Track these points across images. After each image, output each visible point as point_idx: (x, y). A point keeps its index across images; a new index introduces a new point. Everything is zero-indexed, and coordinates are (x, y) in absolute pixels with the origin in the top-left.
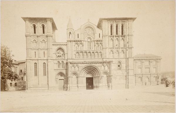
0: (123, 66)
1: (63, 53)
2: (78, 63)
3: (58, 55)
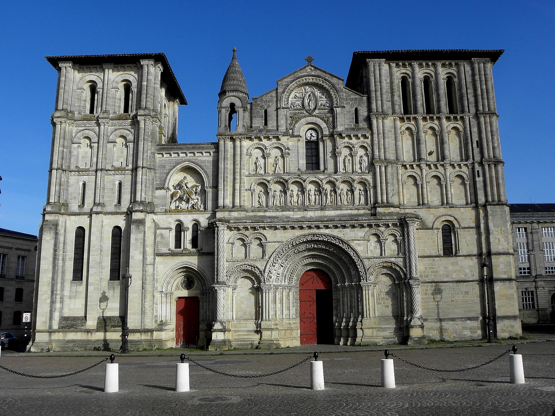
0: (467, 242)
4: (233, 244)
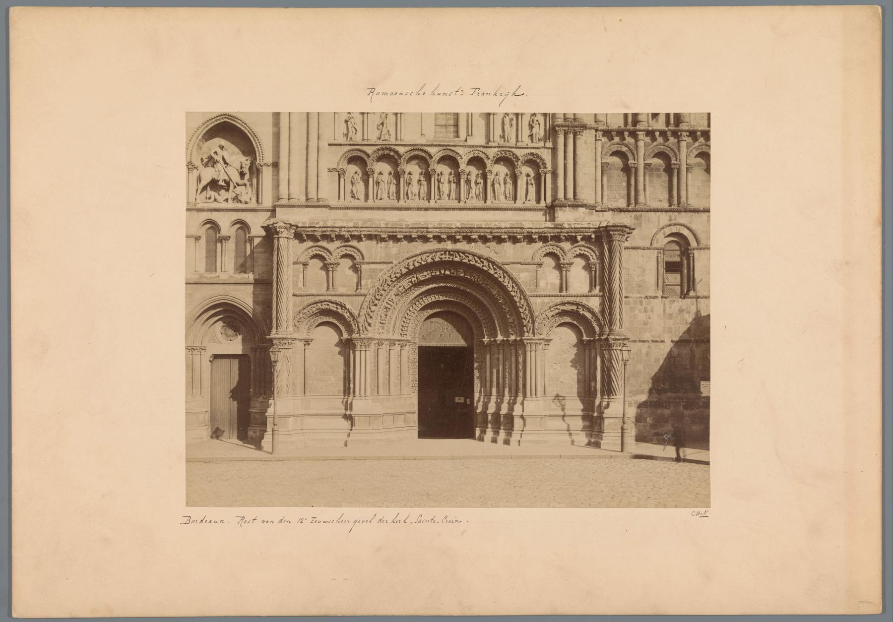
1: (246, 161)
2: (359, 238)
3: (208, 174)
4: (305, 265)
